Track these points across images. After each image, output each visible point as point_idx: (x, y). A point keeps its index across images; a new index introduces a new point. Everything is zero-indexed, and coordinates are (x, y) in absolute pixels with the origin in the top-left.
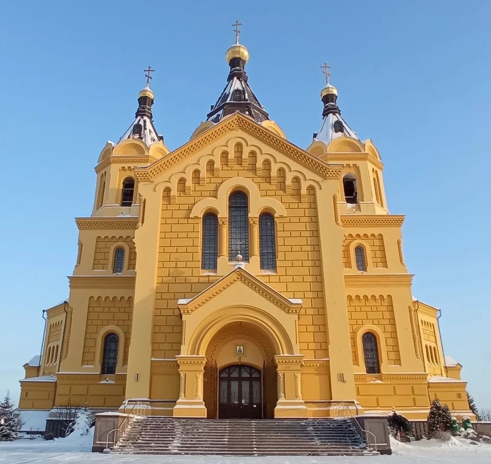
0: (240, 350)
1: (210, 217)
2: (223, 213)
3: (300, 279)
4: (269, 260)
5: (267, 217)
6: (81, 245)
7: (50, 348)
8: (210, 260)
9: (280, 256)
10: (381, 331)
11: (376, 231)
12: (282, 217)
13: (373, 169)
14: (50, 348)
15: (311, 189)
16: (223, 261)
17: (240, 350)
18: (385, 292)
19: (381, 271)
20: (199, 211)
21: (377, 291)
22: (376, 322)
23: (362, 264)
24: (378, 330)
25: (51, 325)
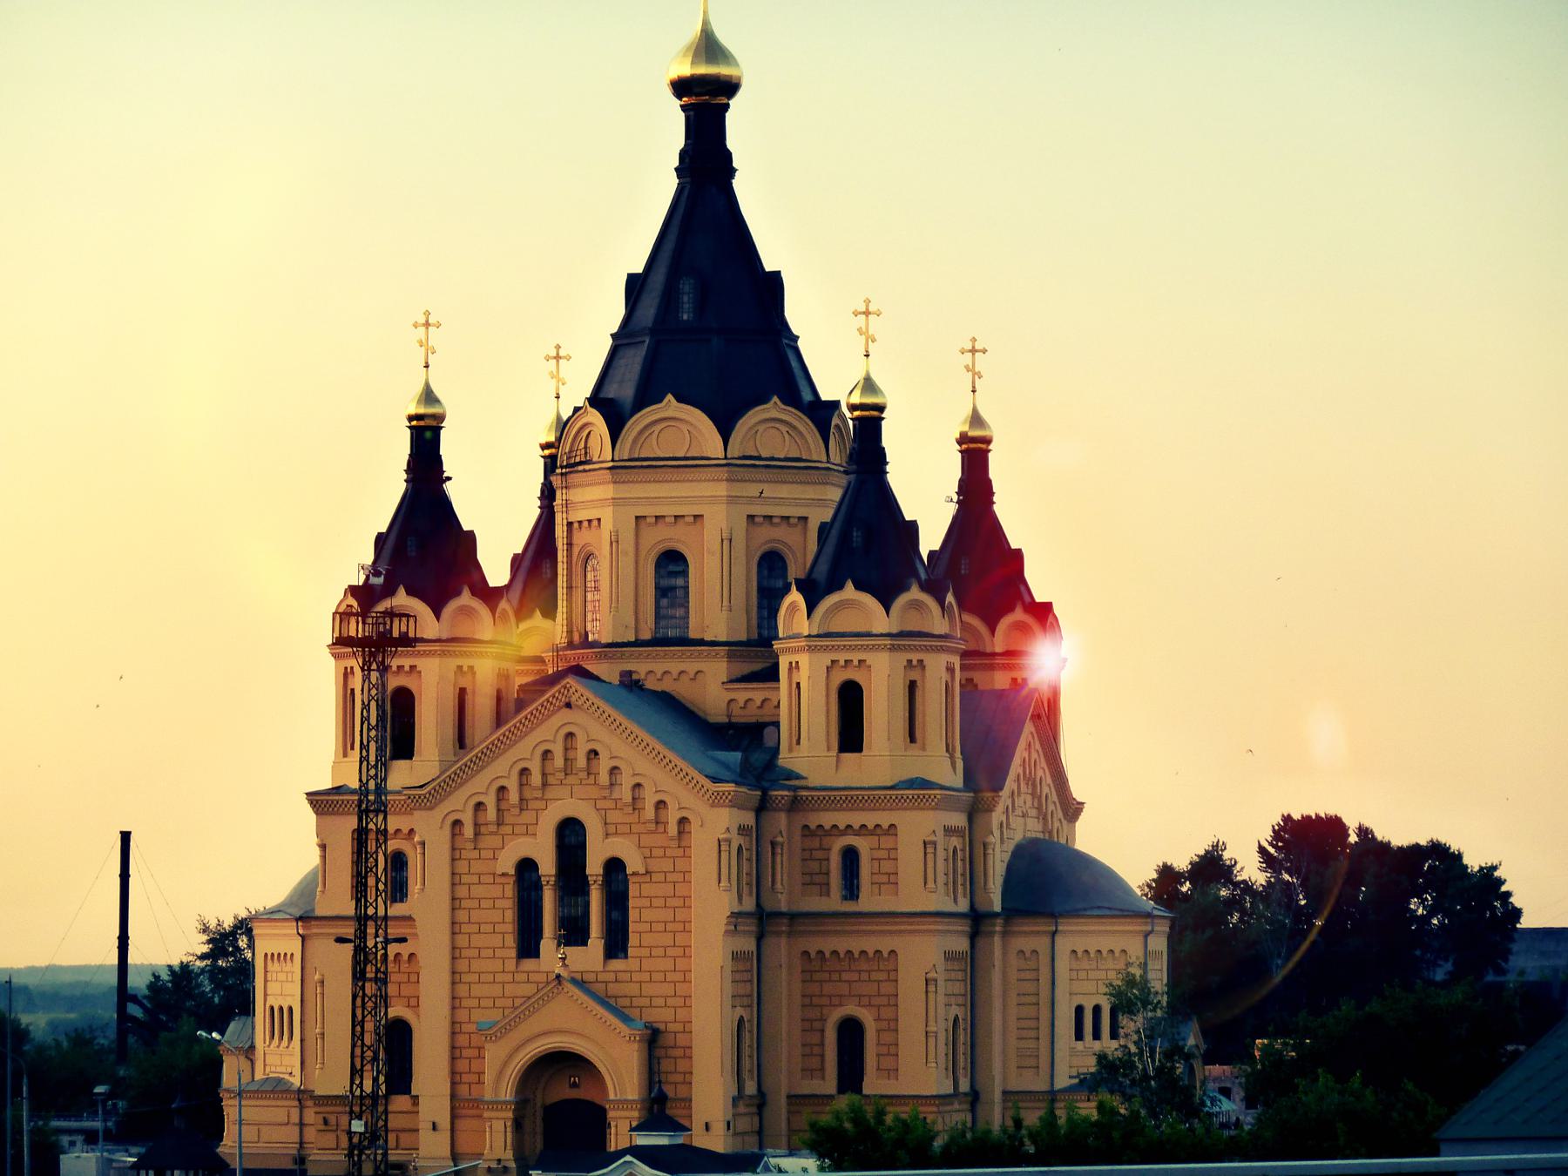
0: (575, 1081)
1: (527, 867)
2: (547, 866)
3: (656, 977)
4: (616, 945)
5: (614, 867)
6: (323, 847)
7: (272, 1008)
8: (528, 946)
9: (633, 940)
10: (871, 1019)
11: (884, 819)
12: (634, 874)
13: (910, 661)
14: (272, 1008)
15: (683, 821)
16: (547, 944)
17: (575, 1081)
18: (885, 944)
19: (885, 903)
20: (507, 863)
21: (870, 944)
22: (865, 1001)
23: (851, 888)
24: (867, 1017)
25: (266, 955)
